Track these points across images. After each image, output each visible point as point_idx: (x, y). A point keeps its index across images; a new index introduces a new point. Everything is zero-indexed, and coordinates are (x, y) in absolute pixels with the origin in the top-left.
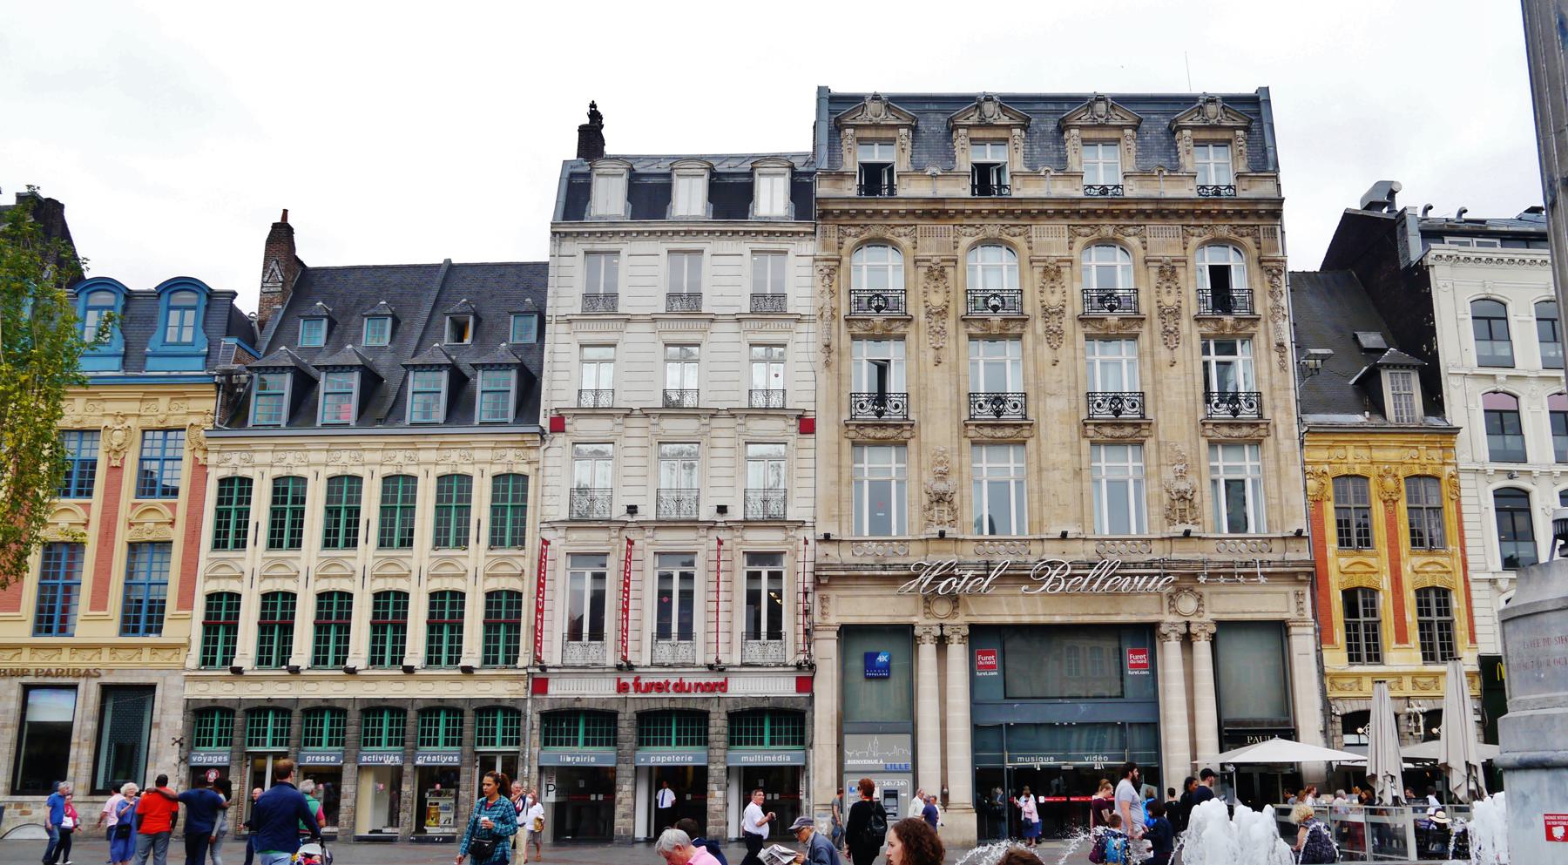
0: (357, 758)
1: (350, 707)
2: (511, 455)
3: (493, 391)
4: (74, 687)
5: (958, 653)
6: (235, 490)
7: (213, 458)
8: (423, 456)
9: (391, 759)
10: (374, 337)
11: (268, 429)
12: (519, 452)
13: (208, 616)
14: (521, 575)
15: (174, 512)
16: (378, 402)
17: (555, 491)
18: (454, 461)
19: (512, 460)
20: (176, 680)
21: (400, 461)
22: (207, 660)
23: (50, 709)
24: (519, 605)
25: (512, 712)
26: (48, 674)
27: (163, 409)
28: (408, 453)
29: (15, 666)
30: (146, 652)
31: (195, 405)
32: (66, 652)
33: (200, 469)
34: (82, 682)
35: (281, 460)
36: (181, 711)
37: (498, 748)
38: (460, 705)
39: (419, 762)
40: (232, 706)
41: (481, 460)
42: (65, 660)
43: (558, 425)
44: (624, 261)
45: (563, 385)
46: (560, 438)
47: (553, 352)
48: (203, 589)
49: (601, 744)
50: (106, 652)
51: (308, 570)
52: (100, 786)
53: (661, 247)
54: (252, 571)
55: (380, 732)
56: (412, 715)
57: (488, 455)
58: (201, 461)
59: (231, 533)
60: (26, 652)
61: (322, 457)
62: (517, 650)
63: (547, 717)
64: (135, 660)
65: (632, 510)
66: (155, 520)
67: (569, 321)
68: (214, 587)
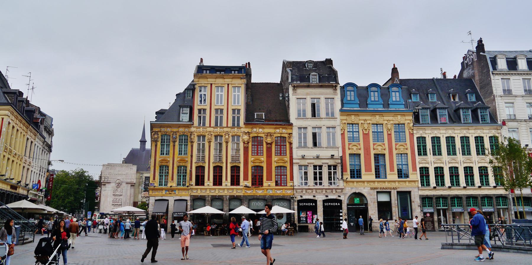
0: (467, 210)
2: (493, 131)
4: (389, 193)
6: (422, 140)
8: (470, 131)
10: (433, 99)
11: (426, 124)
13: (420, 173)
16: (455, 118)
18: (479, 133)
20: (416, 190)
22: (423, 185)
23: (384, 198)
26: (384, 188)
27: (400, 119)
30: (407, 183)
31: (407, 118)
32: (387, 183)
33: (412, 135)
42: (387, 185)
43: (504, 123)
44: (512, 81)
46: (504, 127)
48: (418, 166)
51: (445, 161)
53: (521, 77)
54: (431, 161)
56: (479, 199)
57: (487, 131)
59: (422, 151)
60: (376, 183)
61: (444, 131)
68: (421, 165)
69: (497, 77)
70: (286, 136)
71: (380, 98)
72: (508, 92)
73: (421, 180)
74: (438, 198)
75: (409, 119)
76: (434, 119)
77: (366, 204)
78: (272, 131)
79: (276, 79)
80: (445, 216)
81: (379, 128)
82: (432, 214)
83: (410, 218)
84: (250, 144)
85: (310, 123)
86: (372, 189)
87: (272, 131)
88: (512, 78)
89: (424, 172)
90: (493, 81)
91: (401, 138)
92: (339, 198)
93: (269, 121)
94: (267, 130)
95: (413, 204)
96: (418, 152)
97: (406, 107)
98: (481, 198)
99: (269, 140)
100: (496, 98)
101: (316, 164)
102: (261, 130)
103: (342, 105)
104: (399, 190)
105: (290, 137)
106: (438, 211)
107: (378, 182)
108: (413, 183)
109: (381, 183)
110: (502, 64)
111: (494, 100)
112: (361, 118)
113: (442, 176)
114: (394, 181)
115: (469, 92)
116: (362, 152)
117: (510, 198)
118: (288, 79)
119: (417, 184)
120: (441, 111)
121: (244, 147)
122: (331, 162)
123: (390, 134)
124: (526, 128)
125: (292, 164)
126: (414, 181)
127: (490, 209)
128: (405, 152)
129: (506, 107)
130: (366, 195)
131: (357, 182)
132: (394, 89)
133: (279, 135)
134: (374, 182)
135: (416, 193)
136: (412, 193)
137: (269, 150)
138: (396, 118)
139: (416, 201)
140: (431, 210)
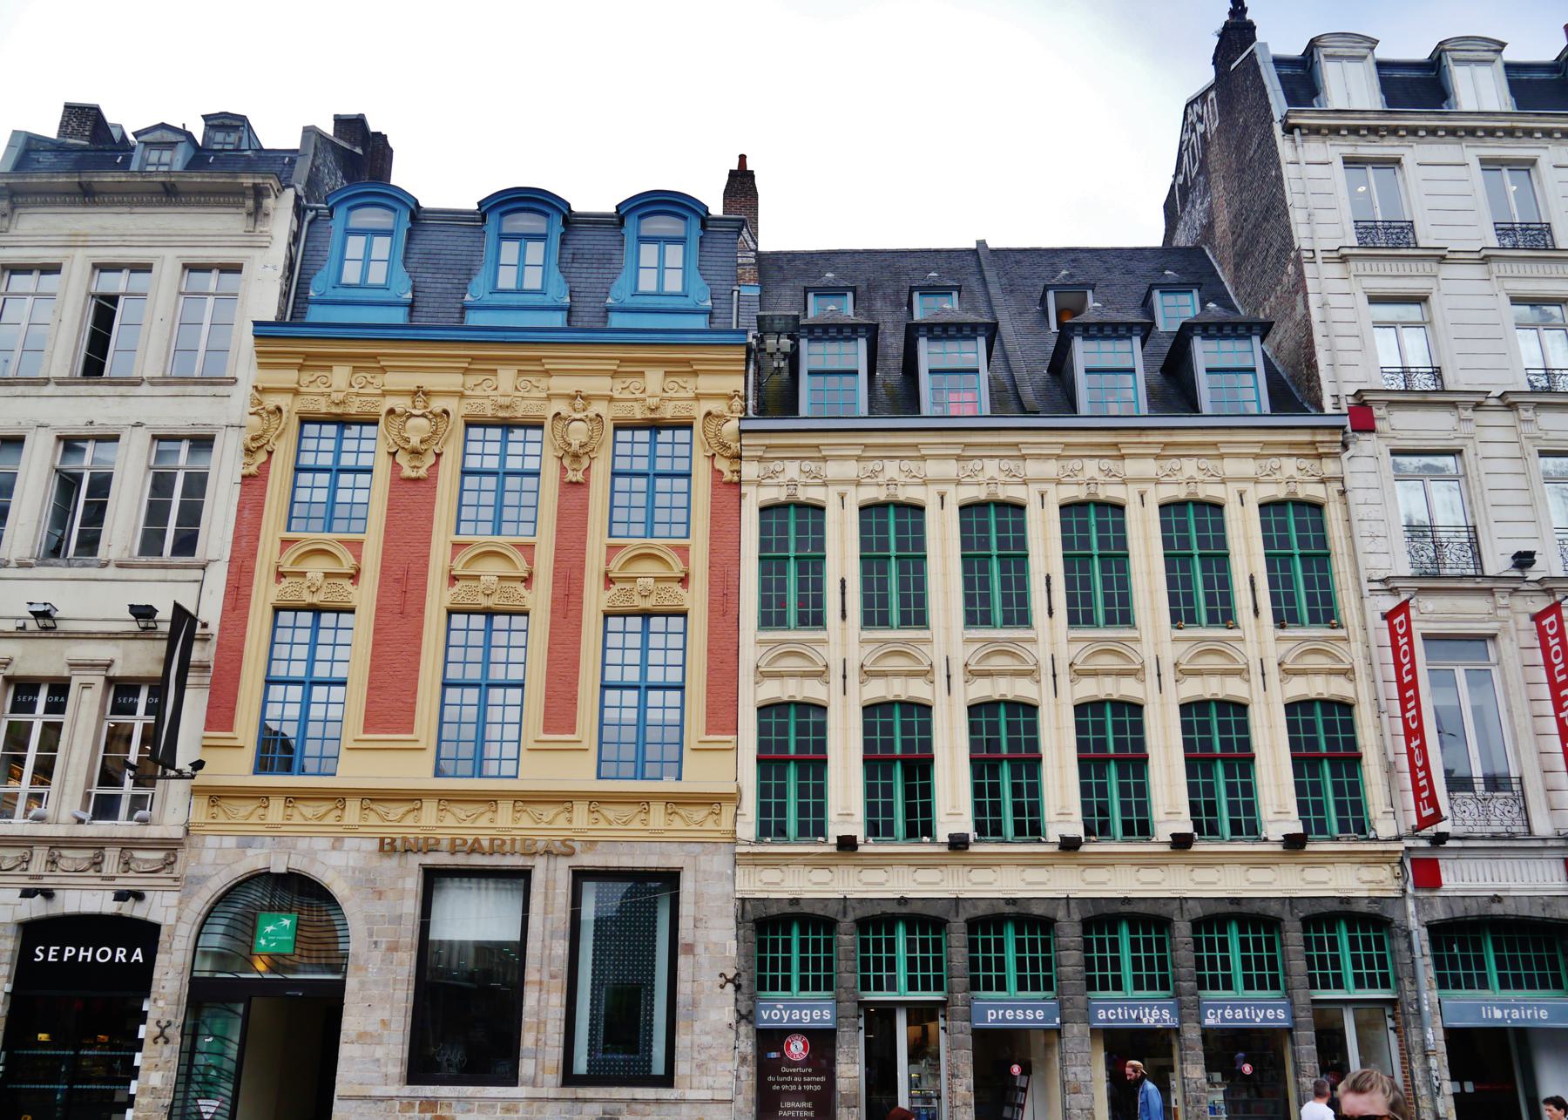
0: (1087, 1014)
1: (1061, 914)
2: (1290, 466)
4: (522, 876)
6: (794, 525)
7: (750, 470)
8: (1131, 468)
9: (1154, 1014)
12: (1305, 463)
13: (763, 745)
14: (1349, 673)
15: (686, 562)
17: (1379, 528)
18: (1190, 477)
19: (1291, 477)
20: (719, 862)
21: (1091, 477)
22: (771, 826)
23: (473, 918)
24: (1349, 726)
25: (1370, 923)
26: (475, 849)
27: (654, 389)
28: (1106, 464)
29: (412, 833)
30: (657, 810)
31: (706, 384)
32: (505, 808)
33: (729, 490)
34: (540, 868)
35: (874, 474)
36: (732, 923)
37: (903, 994)
38: (1274, 910)
39: (1210, 1021)
40: (830, 912)
41: (1244, 480)
43: (1362, 416)
45: (1354, 358)
46: (1365, 444)
47: (1324, 305)
49: (1531, 986)
50: (581, 809)
52: (581, 1066)
53: (1471, 152)
54: (843, 668)
55: (1116, 964)
57: (1249, 467)
58: (728, 476)
59: (794, 596)
61: (950, 469)
62: (1358, 807)
63: (1440, 933)
64: (636, 824)
65: (1524, 560)
67: (1344, 259)
68: (773, 691)
69: (1315, 149)
71: (555, 274)
72: (1388, 238)
73: (763, 791)
74: (878, 922)
76: (900, 396)
77: (339, 964)
80: (921, 1050)
81: (513, 448)
82: (822, 1042)
83: (658, 1068)
86: (388, 848)
88: (1412, 153)
90: (1288, 172)
91: (660, 515)
92: (130, 909)
95: (682, 960)
96: (765, 602)
98: (1196, 925)
100: (1308, 270)
101: (22, 669)
104: (588, 860)
106: (879, 1020)
107: (447, 798)
108: (700, 813)
109: (460, 811)
110: (1350, 88)
111: (1300, 285)
112: (394, 380)
113: (920, 768)
114: (563, 799)
117: (1413, 923)
119: (726, 824)
122: (141, 659)
123: (581, 485)
124: (1514, 450)
126: (711, 801)
127: (1259, 1010)
128: (669, 603)
129: (1379, 325)
130: (339, 889)
131: (293, 797)
135: (720, 888)
136: (687, 886)
138: (636, 383)
139: (710, 941)
140: (815, 1011)
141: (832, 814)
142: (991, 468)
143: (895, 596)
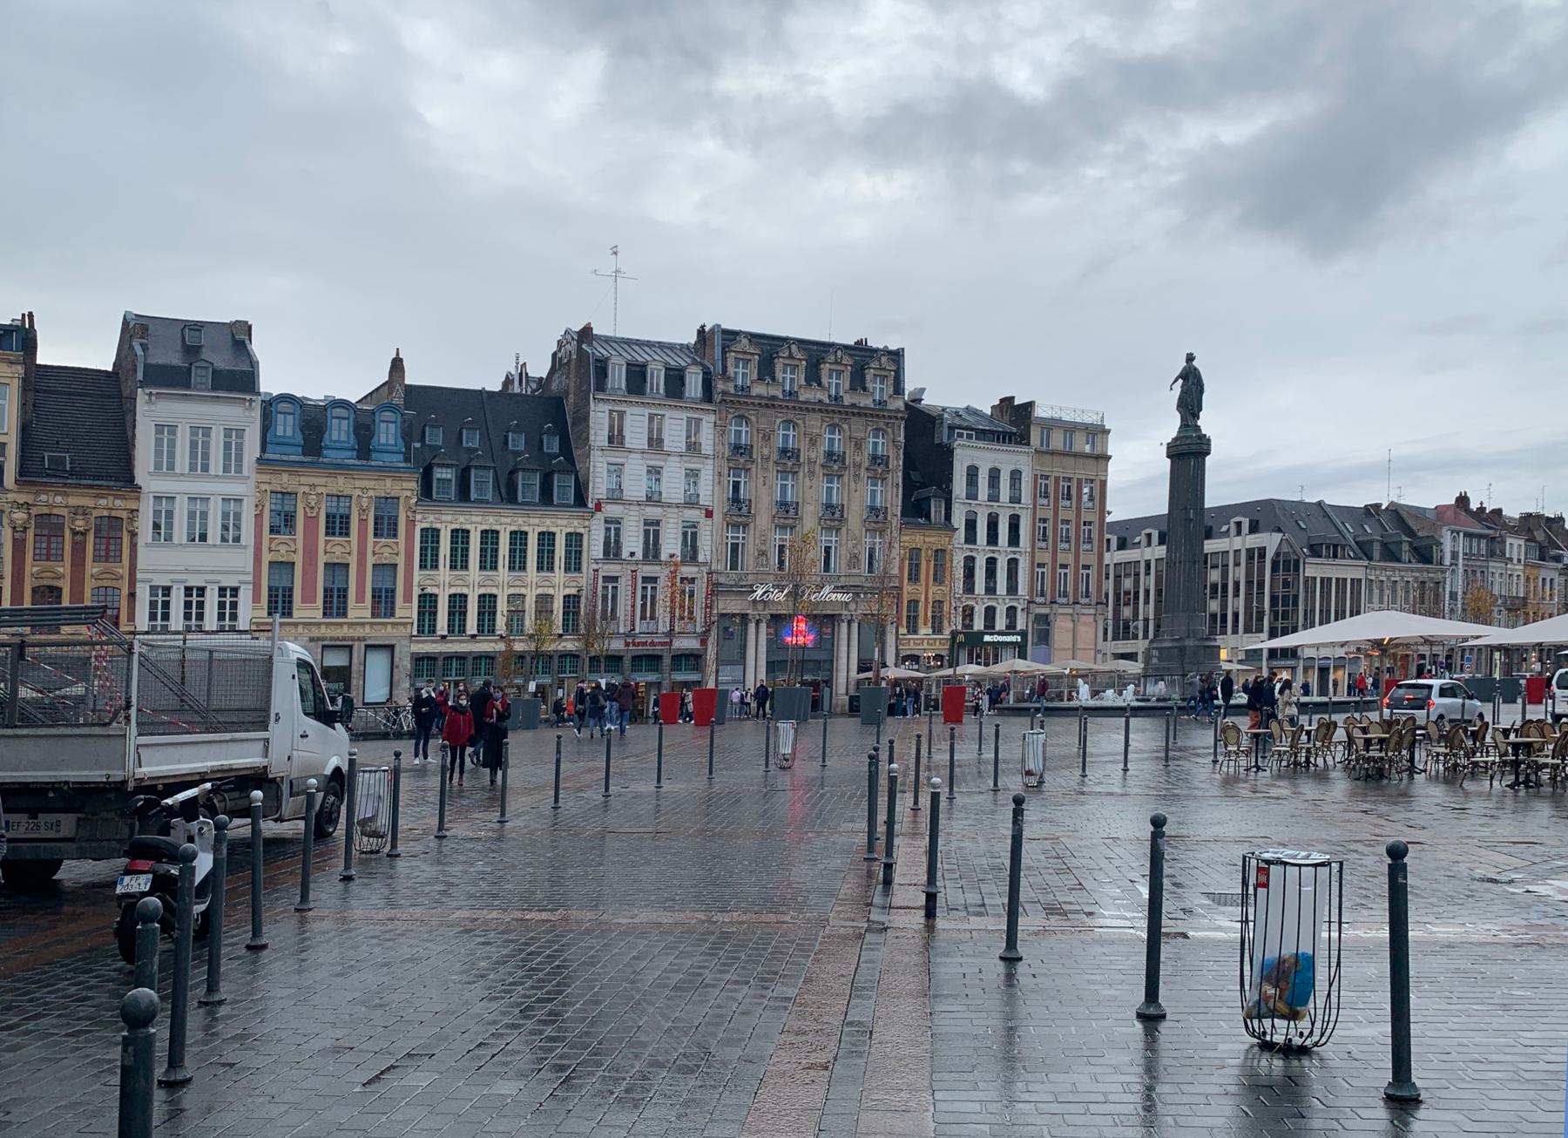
2: (576, 522)
3: (563, 485)
4: (351, 647)
5: (763, 626)
6: (431, 536)
8: (532, 521)
18: (548, 524)
19: (575, 526)
20: (406, 642)
22: (421, 631)
33: (411, 523)
41: (561, 525)
42: (345, 631)
43: (598, 507)
46: (598, 515)
54: (443, 582)
59: (429, 560)
66: (381, 550)
70: (124, 515)
75: (407, 489)
78: (87, 502)
79: (102, 358)
84: (30, 534)
85: (181, 487)
87: (87, 502)
89: (428, 603)
93: (81, 476)
94: (73, 501)
97: (407, 460)
99: (80, 524)
102: (59, 499)
103: (263, 450)
105: (131, 520)
111: (588, 456)
114: (363, 624)
115: (548, 432)
116: (298, 560)
118: (135, 370)
120: (481, 473)
121: (15, 540)
125: (133, 581)
126: (404, 624)
132: (387, 415)
133: (106, 513)
134: (319, 624)
137: (79, 549)
141: (439, 627)
142: (491, 519)
143: (459, 560)
